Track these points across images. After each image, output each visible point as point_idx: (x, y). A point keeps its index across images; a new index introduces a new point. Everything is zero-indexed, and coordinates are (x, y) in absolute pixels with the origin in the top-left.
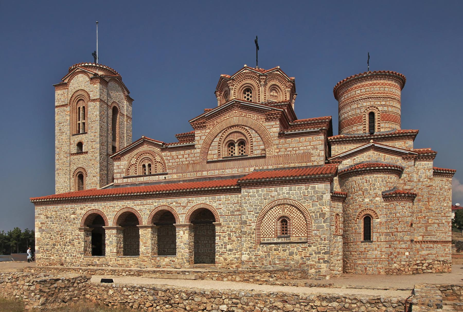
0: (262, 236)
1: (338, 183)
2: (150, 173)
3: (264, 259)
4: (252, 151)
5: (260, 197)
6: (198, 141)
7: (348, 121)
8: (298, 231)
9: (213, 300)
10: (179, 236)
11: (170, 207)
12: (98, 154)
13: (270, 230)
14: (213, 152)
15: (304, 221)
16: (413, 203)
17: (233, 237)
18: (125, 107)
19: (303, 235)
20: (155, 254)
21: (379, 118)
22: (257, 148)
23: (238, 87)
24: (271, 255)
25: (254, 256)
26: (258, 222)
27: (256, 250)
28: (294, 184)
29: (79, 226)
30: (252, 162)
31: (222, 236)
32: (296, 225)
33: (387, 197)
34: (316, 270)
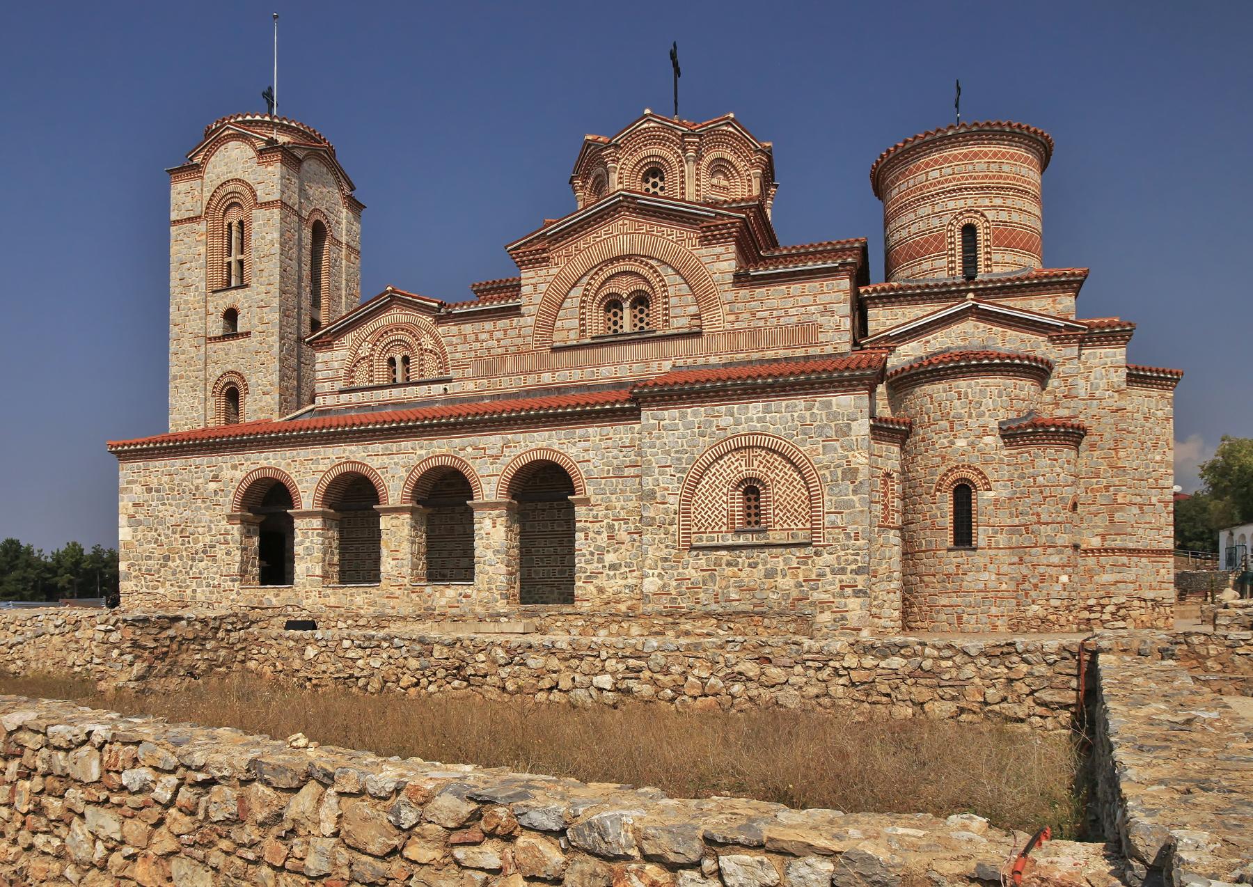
0: (695, 529)
1: (887, 402)
2: (408, 379)
4: (667, 321)
6: (529, 296)
7: (910, 248)
8: (788, 515)
9: (575, 662)
10: (482, 532)
11: (459, 459)
12: (276, 338)
13: (716, 512)
14: (567, 324)
15: (803, 490)
16: (1078, 451)
17: (621, 532)
18: (343, 223)
19: (800, 526)
20: (420, 579)
21: (987, 240)
22: (679, 311)
23: (630, 165)
24: (718, 578)
27: (680, 565)
28: (777, 396)
29: (228, 510)
30: (668, 346)
32: (781, 500)
33: (1012, 435)
34: (834, 616)
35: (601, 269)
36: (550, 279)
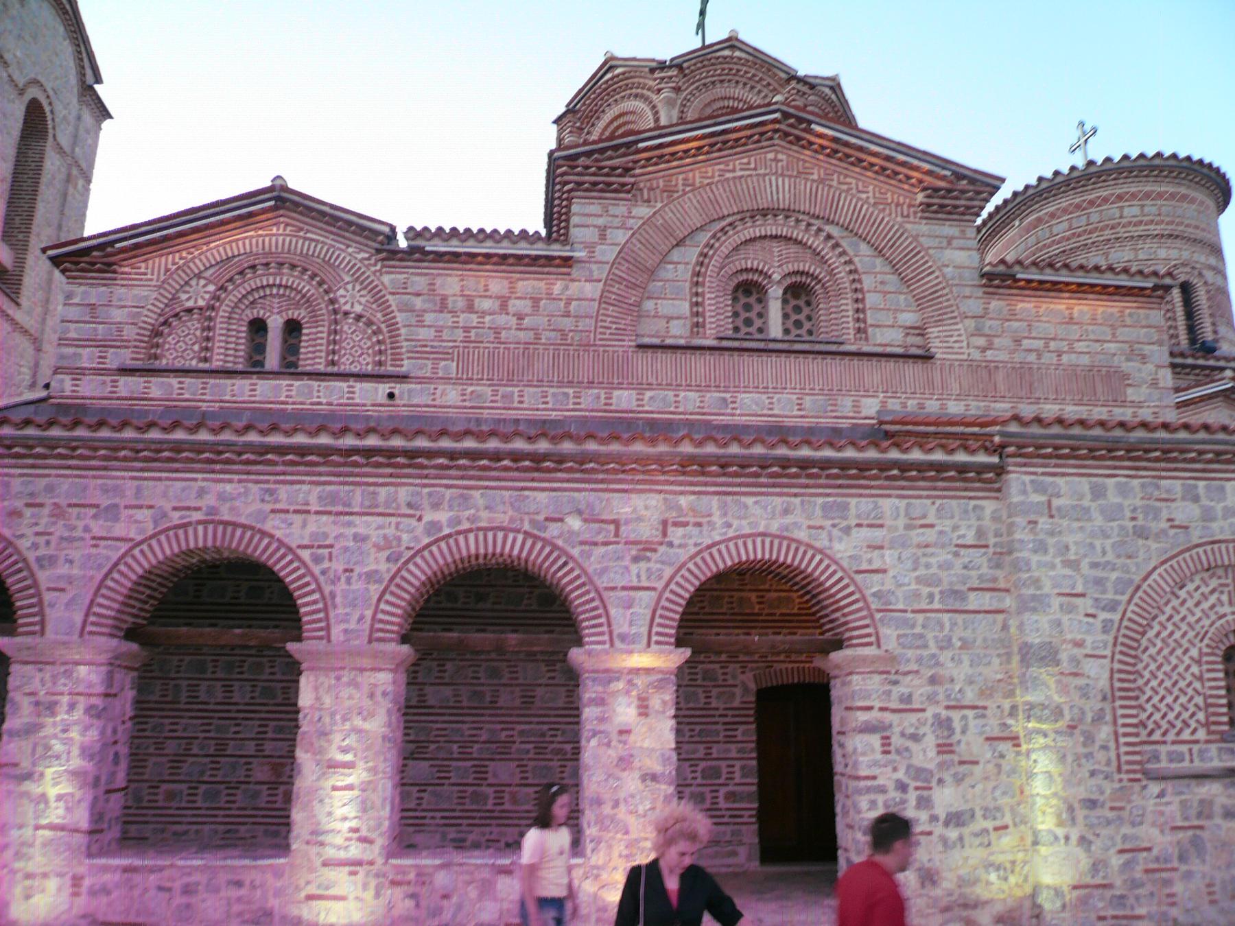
3: (1174, 870)
6: (590, 247)
14: (666, 307)
26: (1118, 657)
31: (897, 730)
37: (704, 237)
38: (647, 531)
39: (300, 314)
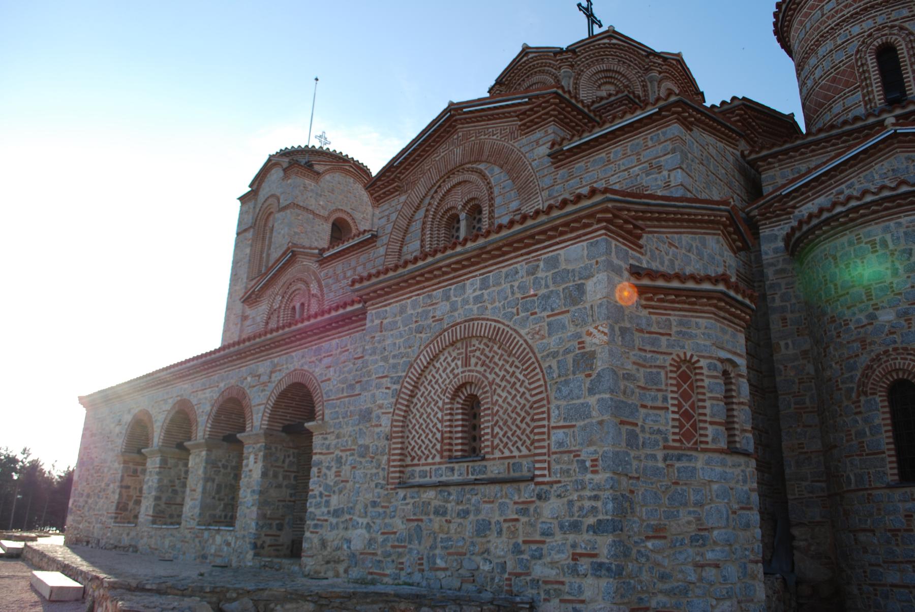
5: (406, 328)
25: (383, 534)
32: (501, 413)
35: (440, 186)
36: (399, 207)
37: (427, 201)
38: (264, 378)
39: (303, 300)
